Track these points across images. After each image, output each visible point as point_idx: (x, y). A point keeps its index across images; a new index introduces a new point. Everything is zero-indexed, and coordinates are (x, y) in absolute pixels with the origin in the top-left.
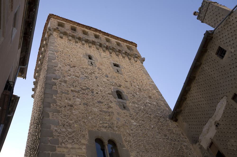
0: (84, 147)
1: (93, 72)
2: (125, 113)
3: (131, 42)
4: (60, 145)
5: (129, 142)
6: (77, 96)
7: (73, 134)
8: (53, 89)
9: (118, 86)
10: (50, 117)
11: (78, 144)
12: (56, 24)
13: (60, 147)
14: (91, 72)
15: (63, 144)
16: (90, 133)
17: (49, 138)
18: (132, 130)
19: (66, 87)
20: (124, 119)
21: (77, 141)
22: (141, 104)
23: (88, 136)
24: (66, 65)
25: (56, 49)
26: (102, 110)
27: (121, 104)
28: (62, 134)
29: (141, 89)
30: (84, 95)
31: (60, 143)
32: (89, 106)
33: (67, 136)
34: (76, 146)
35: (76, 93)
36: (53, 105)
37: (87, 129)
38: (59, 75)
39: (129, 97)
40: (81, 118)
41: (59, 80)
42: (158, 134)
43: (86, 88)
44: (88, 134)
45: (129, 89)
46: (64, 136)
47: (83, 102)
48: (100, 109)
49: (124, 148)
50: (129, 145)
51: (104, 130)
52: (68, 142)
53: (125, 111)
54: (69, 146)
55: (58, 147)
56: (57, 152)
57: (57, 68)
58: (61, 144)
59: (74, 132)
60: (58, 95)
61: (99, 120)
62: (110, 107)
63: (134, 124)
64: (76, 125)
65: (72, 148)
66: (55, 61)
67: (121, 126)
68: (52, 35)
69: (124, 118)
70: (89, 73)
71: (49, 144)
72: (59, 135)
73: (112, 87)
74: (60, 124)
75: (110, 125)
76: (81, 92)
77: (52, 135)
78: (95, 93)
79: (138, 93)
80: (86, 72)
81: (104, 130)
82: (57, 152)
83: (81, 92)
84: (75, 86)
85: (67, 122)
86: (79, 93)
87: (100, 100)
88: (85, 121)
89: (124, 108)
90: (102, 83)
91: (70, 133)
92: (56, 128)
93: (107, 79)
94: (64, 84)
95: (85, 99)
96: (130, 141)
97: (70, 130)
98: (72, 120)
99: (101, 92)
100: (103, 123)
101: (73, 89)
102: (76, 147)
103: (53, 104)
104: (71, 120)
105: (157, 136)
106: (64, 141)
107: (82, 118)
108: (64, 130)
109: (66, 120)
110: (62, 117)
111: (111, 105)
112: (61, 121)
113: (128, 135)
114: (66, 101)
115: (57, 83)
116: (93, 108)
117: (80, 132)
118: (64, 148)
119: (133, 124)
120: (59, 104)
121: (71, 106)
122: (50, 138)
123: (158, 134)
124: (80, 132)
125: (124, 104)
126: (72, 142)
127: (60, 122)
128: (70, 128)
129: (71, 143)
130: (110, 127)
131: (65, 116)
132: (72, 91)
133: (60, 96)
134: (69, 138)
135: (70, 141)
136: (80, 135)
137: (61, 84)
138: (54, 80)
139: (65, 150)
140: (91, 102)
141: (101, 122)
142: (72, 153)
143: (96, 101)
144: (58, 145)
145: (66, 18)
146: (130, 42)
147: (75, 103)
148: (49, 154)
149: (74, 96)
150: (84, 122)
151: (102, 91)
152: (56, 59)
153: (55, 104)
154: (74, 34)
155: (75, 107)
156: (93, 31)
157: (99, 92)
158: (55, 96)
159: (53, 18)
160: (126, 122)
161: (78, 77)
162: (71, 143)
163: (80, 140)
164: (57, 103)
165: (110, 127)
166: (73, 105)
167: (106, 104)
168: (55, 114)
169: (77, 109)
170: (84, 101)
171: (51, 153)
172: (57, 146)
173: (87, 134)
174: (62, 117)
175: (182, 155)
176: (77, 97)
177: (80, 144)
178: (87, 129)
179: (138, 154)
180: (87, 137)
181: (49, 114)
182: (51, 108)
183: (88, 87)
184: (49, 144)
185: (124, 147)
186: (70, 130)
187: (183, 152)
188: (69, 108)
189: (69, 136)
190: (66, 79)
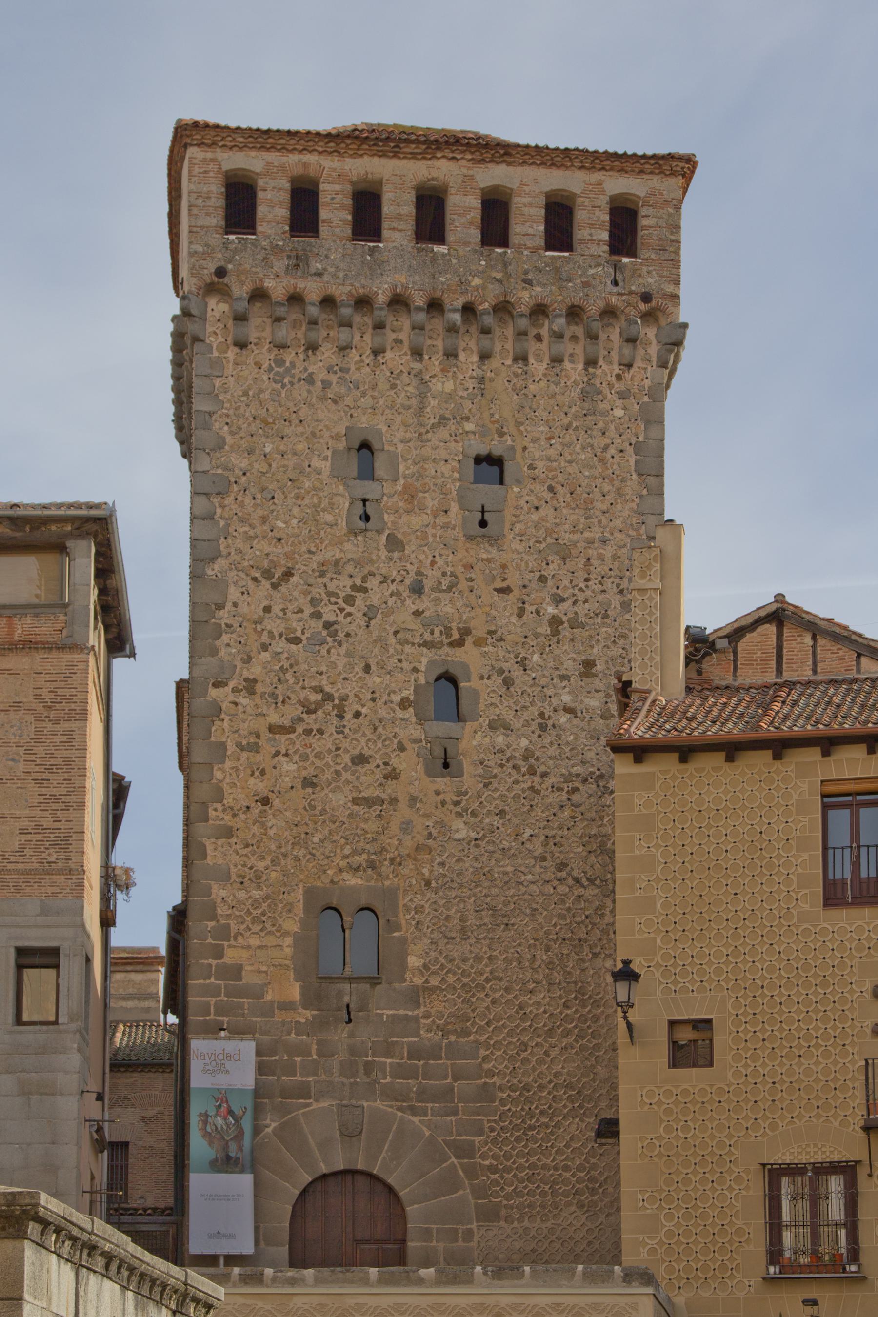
0: (289, 941)
1: (364, 579)
2: (438, 793)
3: (654, 156)
4: (232, 942)
5: (419, 909)
6: (284, 751)
7: (265, 906)
8: (213, 739)
9: (451, 644)
10: (209, 857)
11: (274, 934)
12: (214, 222)
13: (235, 947)
14: (354, 587)
15: (240, 938)
16: (309, 893)
17: (209, 923)
18: (442, 864)
19: (251, 718)
20: (427, 824)
21: (274, 925)
22: (527, 724)
23: (301, 907)
24: (255, 579)
25: (220, 471)
26: (363, 794)
27: (439, 752)
28: (237, 910)
29: (562, 623)
30: (310, 738)
31: (232, 935)
32: (319, 788)
33: (251, 913)
34: (270, 941)
35: (282, 738)
36: (216, 810)
37: (301, 886)
38: (230, 654)
39: (483, 696)
40: (290, 847)
41: (232, 684)
42: (534, 866)
43: (319, 697)
44: (302, 902)
45: (501, 640)
46: (242, 913)
47: (304, 773)
48: (355, 794)
49: (396, 934)
50: (414, 923)
51: (352, 881)
52: (250, 930)
53: (442, 783)
54: (254, 942)
55: (230, 946)
56: (225, 960)
57: (224, 616)
58: (235, 939)
59: (267, 897)
60: (228, 764)
61: (343, 841)
62: (393, 775)
63: (461, 836)
64: (273, 875)
65: (259, 947)
66: (216, 567)
67: (408, 855)
68: (202, 341)
69: (427, 816)
70: (340, 601)
71: (210, 940)
72: (229, 912)
73: (425, 658)
74: (234, 877)
75: (373, 857)
76: (300, 729)
77: (214, 917)
78: (348, 716)
79: (536, 658)
80: (330, 594)
81: (352, 881)
82: (225, 960)
83: (300, 729)
84: (283, 702)
85: (251, 868)
86: (292, 736)
87: (363, 748)
88: (301, 853)
89: (446, 765)
90: (385, 648)
91: (256, 904)
92: (223, 893)
93: (414, 608)
94: (244, 701)
95: (312, 759)
96: (423, 907)
97: (256, 894)
98: (263, 858)
99: (373, 700)
100: (355, 852)
101: (274, 718)
102: (269, 945)
103: (216, 805)
104: (260, 860)
105: (525, 874)
106: (243, 927)
107: (292, 844)
108: (242, 895)
109: (249, 859)
110: (238, 854)
111: (394, 762)
112: (236, 866)
113: (423, 883)
114: (252, 781)
115: (224, 708)
116: (330, 795)
117: (281, 897)
118: (242, 947)
119: (457, 836)
120: (231, 800)
121: (265, 801)
122: (211, 924)
123: (534, 866)
124: (281, 897)
125: (449, 745)
126: (261, 930)
127: (233, 870)
128: (259, 887)
129: (257, 933)
130: (372, 865)
131: (247, 846)
132: (272, 729)
133: (233, 768)
134: (254, 920)
135: (256, 928)
136: (280, 905)
137: (236, 704)
138: (213, 693)
139: (245, 954)
140: (330, 767)
141: (347, 850)
142: (261, 960)
143: (347, 759)
144: (229, 941)
145: (264, 127)
146: (644, 156)
147: (278, 788)
148: (210, 965)
149: (277, 754)
150: (297, 859)
151: (377, 695)
152: (220, 555)
153: (219, 806)
154: (301, 285)
155: (276, 802)
156: (414, 156)
157: (363, 706)
158: (219, 769)
159: (198, 145)
160: (430, 834)
161: (296, 641)
162: (257, 933)
163: (280, 921)
164: (225, 802)
165: (372, 865)
166: (271, 795)
167: (378, 766)
168: (220, 842)
169: (281, 812)
170: (306, 768)
171: (214, 962)
172: (226, 943)
173: (299, 901)
174: (238, 854)
175: (585, 936)
176: (286, 755)
177: (278, 934)
178: (301, 886)
179: (434, 946)
180: (299, 909)
181: (205, 846)
182: (211, 822)
183: (328, 693)
184: (210, 940)
185: (398, 928)
186: (256, 894)
187: (594, 924)
188: (257, 809)
189: (254, 912)
190: (255, 671)
